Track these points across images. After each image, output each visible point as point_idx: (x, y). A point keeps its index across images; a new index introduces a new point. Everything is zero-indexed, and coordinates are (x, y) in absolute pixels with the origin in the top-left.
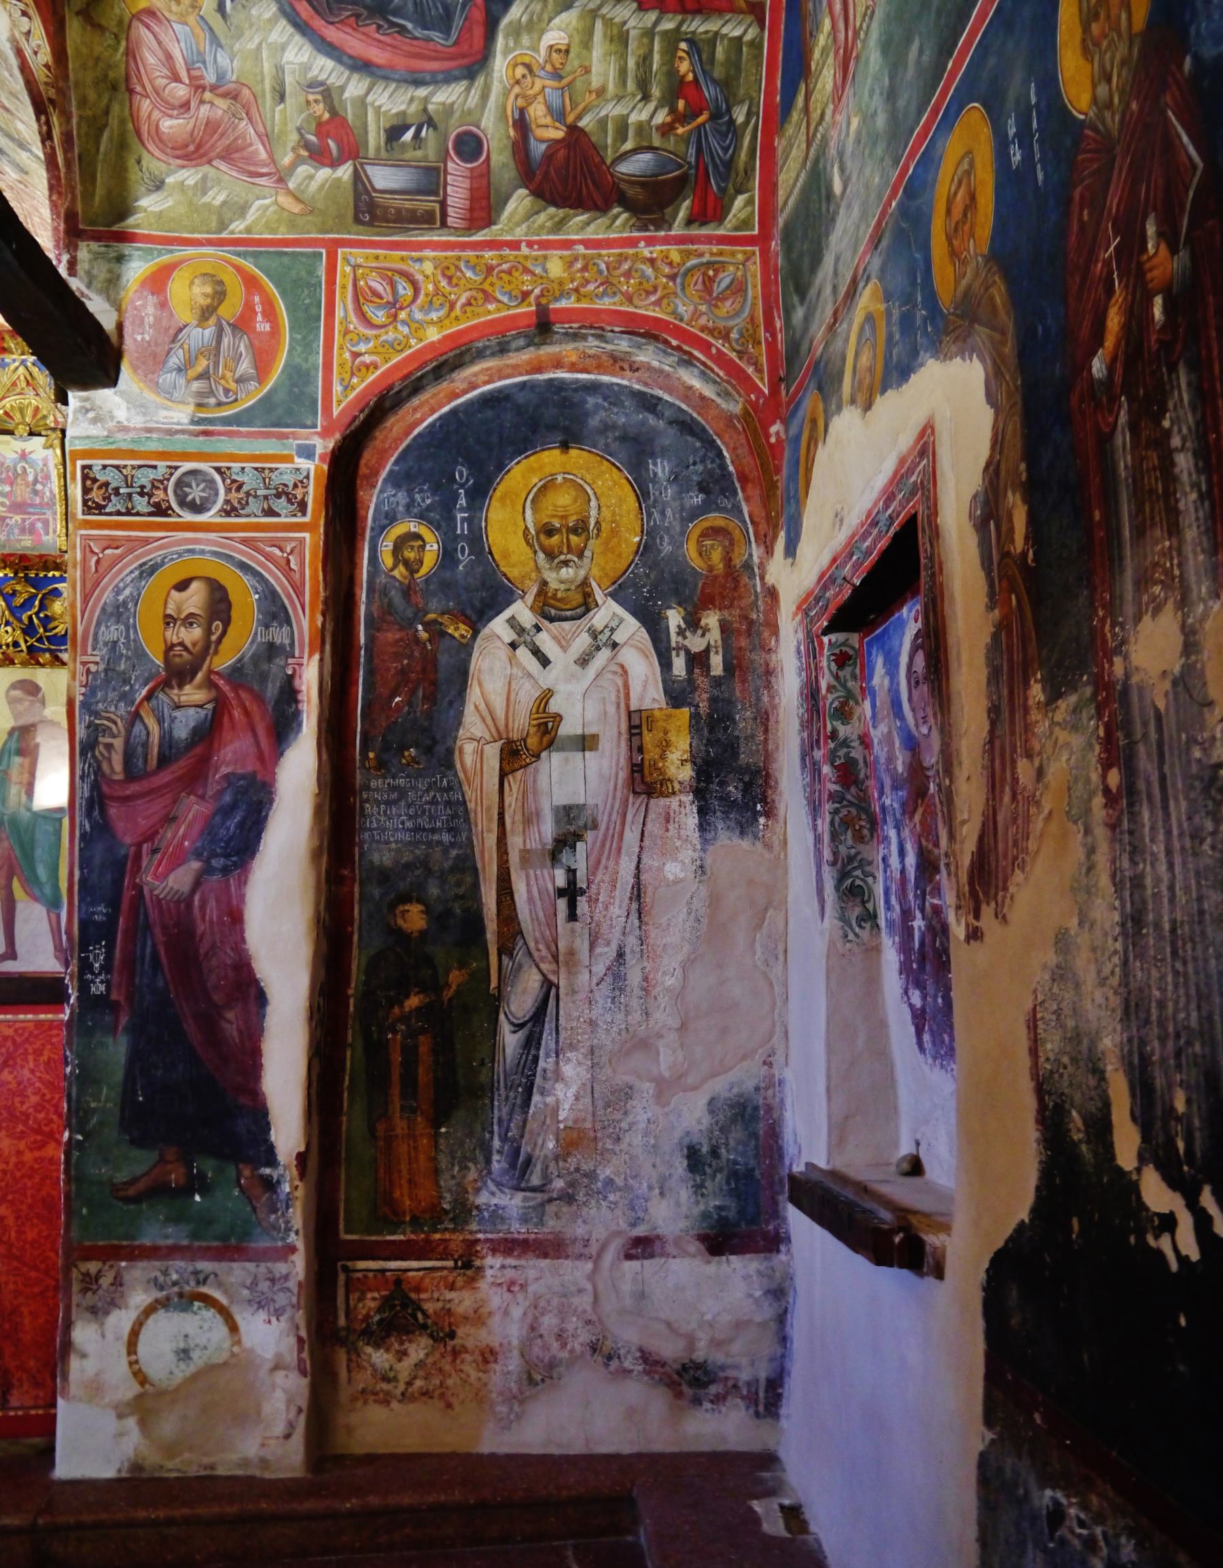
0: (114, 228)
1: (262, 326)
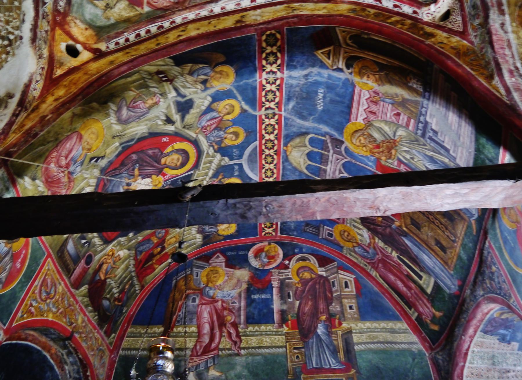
0: (15, 177)
1: (18, 265)
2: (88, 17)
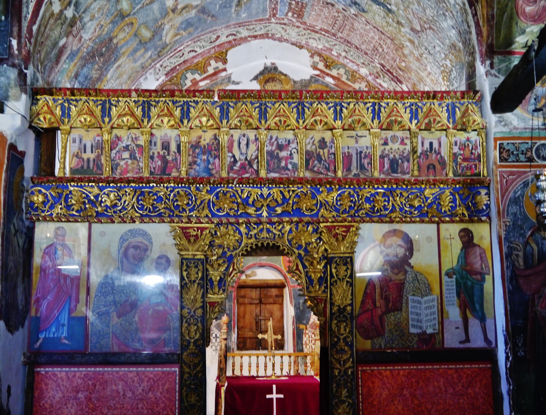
0: (508, 50)
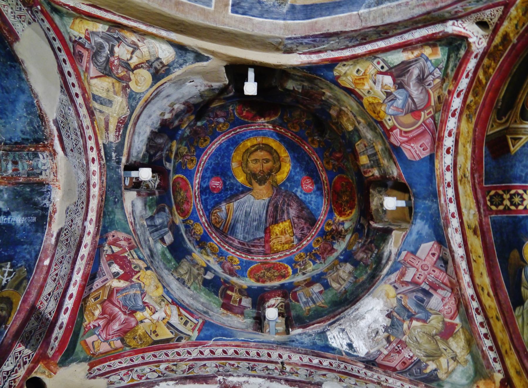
2: (464, 381)
